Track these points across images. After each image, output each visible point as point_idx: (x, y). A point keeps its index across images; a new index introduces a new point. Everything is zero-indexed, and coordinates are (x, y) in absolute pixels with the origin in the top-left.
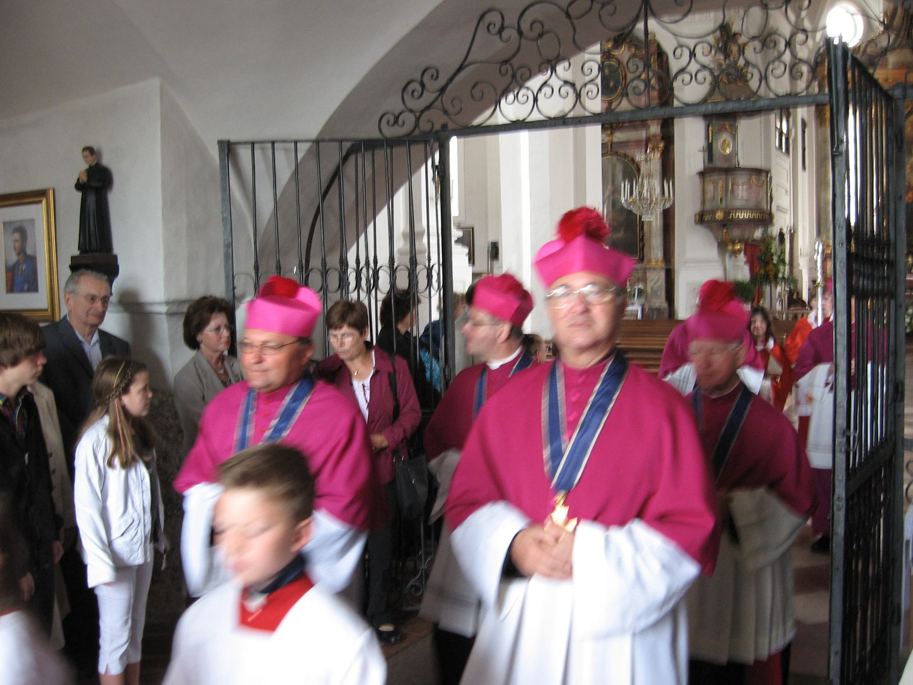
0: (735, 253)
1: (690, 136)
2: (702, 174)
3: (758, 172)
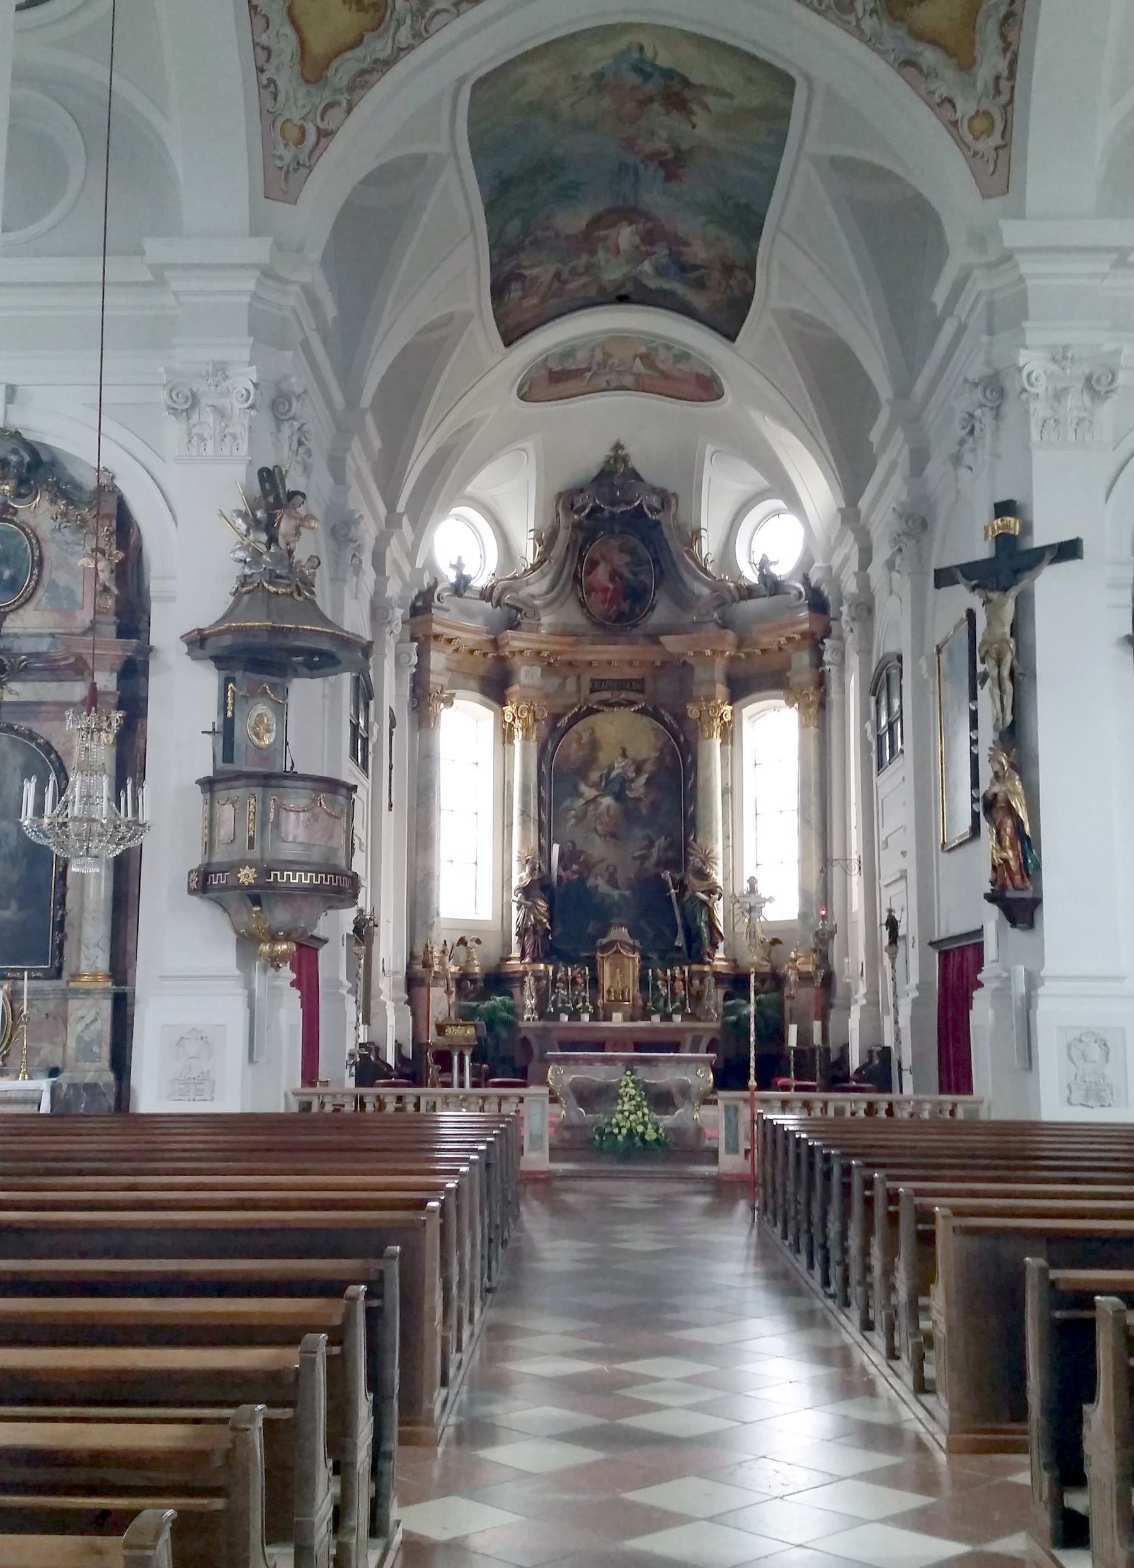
0: (274, 961)
1: (185, 703)
2: (208, 785)
3: (333, 786)
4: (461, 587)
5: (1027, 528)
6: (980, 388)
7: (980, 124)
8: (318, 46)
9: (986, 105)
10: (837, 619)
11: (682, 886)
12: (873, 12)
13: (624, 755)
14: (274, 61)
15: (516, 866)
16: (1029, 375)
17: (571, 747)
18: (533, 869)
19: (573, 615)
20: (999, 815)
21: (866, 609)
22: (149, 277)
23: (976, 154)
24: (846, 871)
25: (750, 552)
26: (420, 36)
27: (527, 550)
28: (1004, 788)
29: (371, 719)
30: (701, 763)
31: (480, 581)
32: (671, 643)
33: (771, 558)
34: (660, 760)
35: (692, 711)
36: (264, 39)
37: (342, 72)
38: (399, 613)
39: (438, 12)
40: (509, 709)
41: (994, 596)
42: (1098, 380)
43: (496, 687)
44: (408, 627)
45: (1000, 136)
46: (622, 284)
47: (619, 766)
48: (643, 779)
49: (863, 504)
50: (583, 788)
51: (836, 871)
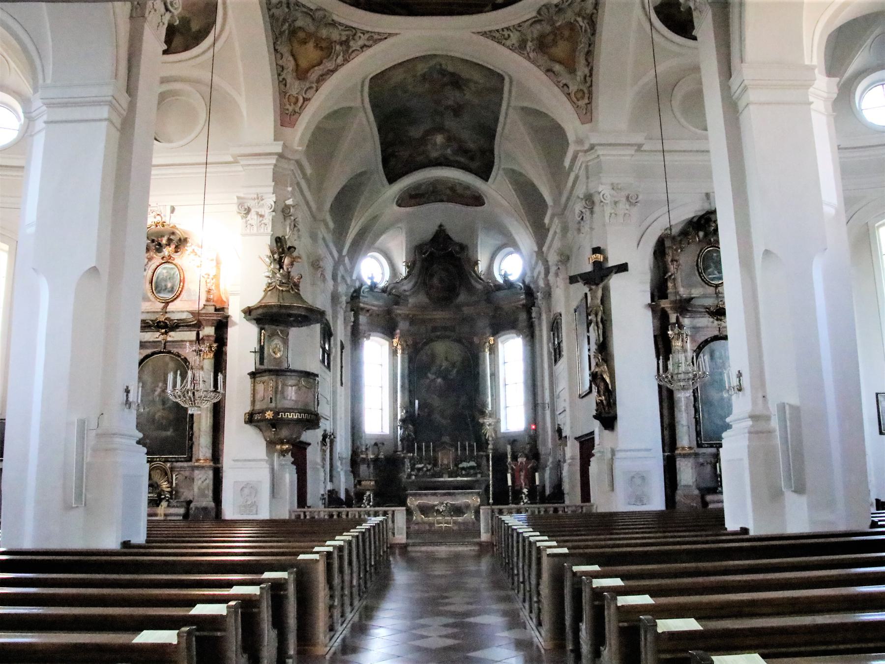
3: (310, 376)
4: (373, 287)
7: (580, 95)
8: (304, 64)
9: (581, 87)
10: (537, 299)
11: (473, 419)
13: (446, 359)
14: (285, 71)
15: (399, 410)
17: (423, 357)
18: (407, 412)
19: (422, 298)
21: (548, 295)
22: (231, 159)
24: (544, 408)
25: (500, 270)
26: (346, 61)
27: (403, 271)
29: (332, 345)
30: (481, 362)
31: (382, 285)
32: (466, 310)
33: (509, 273)
34: (463, 362)
35: (476, 340)
36: (280, 62)
37: (314, 75)
38: (344, 299)
39: (353, 51)
40: (395, 341)
43: (389, 331)
44: (349, 305)
46: (437, 159)
47: (445, 364)
48: (455, 371)
49: (545, 249)
50: (429, 375)
51: (540, 409)
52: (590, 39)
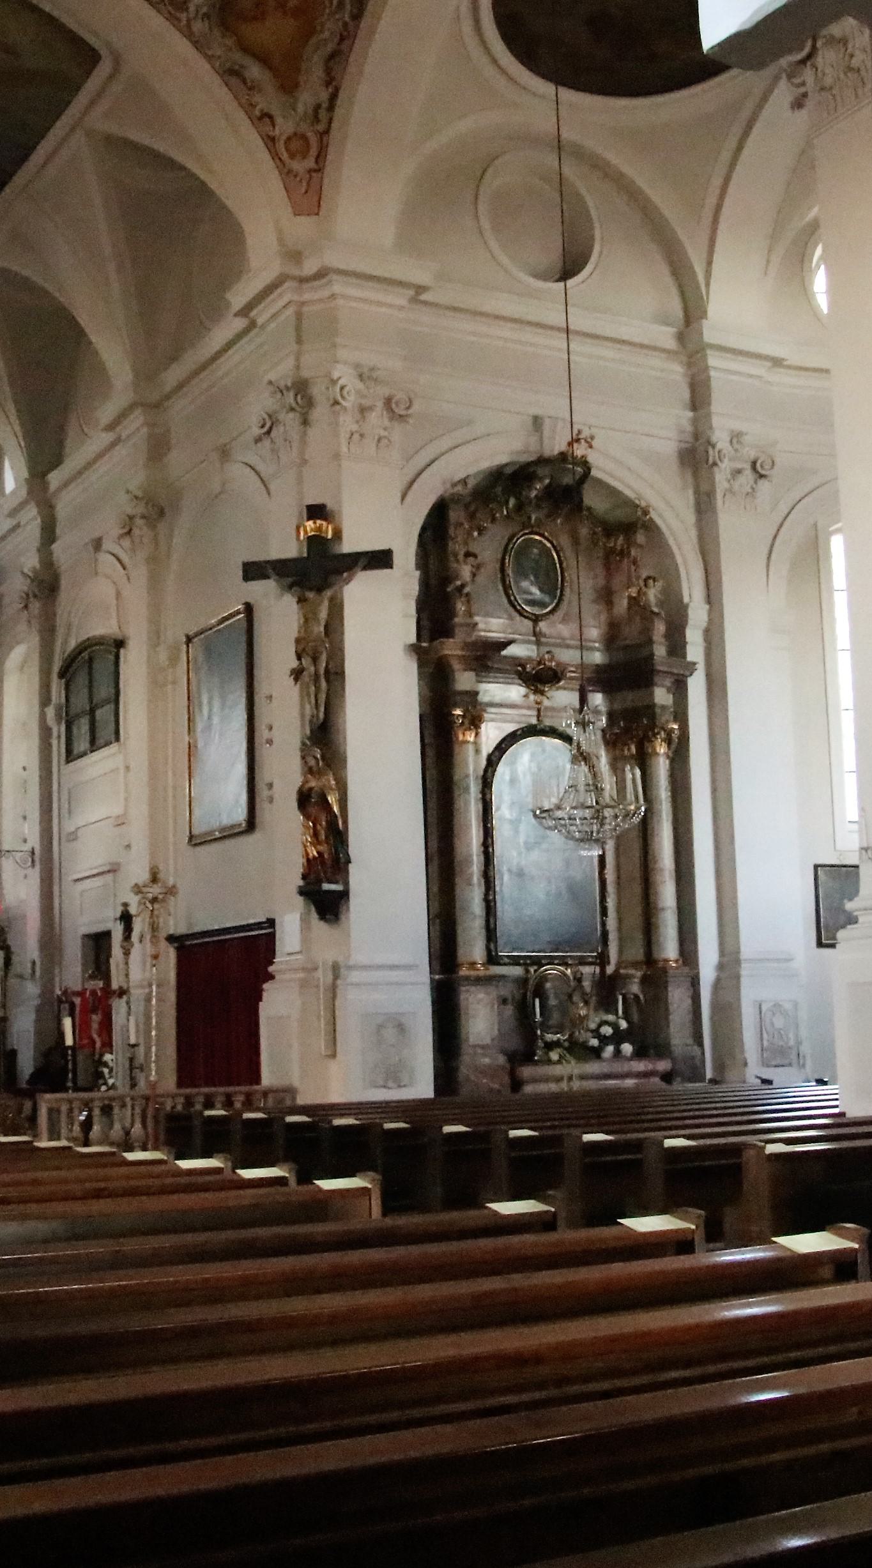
5: (338, 534)
6: (292, 394)
9: (304, 128)
12: (206, 16)
16: (342, 388)
20: (313, 810)
23: (289, 172)
28: (320, 784)
41: (311, 595)
42: (397, 404)
45: (313, 160)
52: (345, 24)
